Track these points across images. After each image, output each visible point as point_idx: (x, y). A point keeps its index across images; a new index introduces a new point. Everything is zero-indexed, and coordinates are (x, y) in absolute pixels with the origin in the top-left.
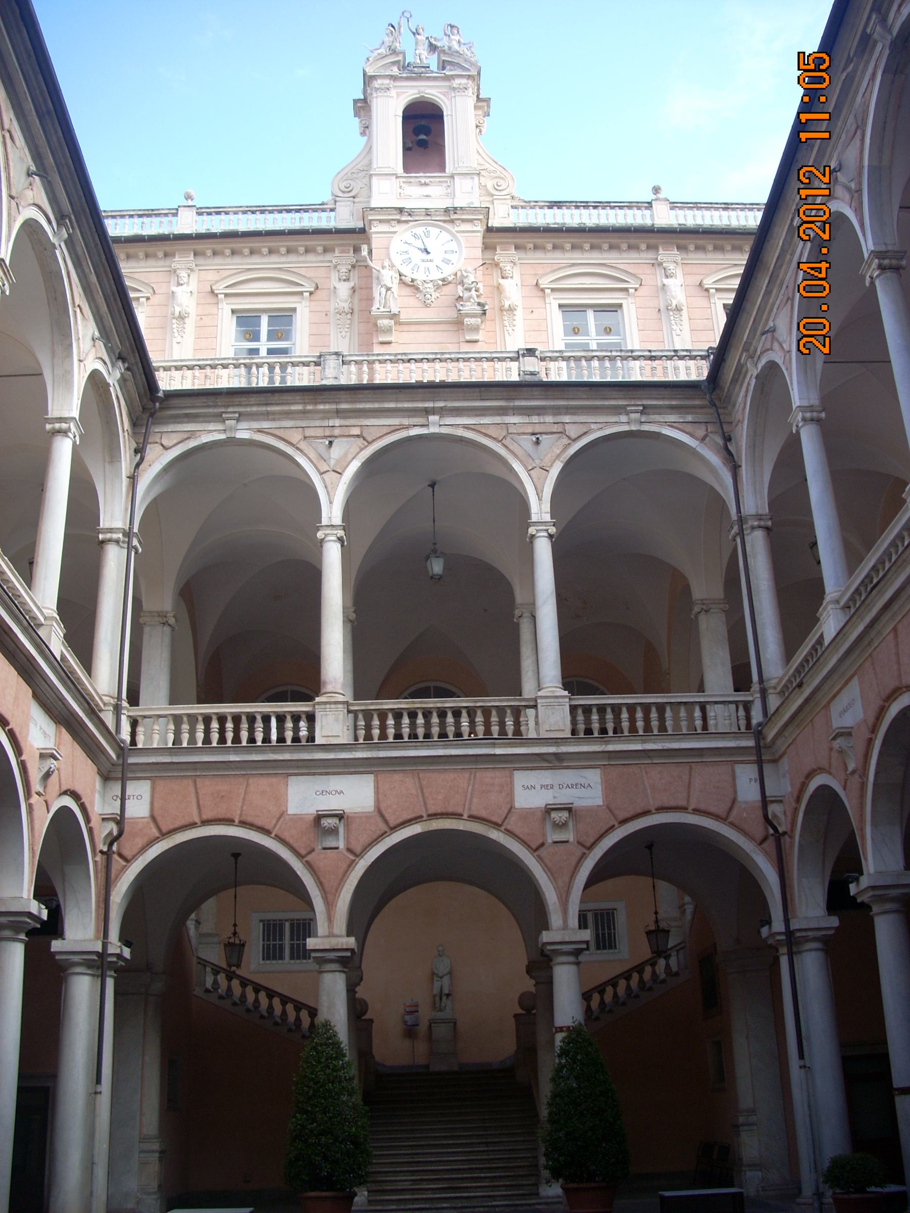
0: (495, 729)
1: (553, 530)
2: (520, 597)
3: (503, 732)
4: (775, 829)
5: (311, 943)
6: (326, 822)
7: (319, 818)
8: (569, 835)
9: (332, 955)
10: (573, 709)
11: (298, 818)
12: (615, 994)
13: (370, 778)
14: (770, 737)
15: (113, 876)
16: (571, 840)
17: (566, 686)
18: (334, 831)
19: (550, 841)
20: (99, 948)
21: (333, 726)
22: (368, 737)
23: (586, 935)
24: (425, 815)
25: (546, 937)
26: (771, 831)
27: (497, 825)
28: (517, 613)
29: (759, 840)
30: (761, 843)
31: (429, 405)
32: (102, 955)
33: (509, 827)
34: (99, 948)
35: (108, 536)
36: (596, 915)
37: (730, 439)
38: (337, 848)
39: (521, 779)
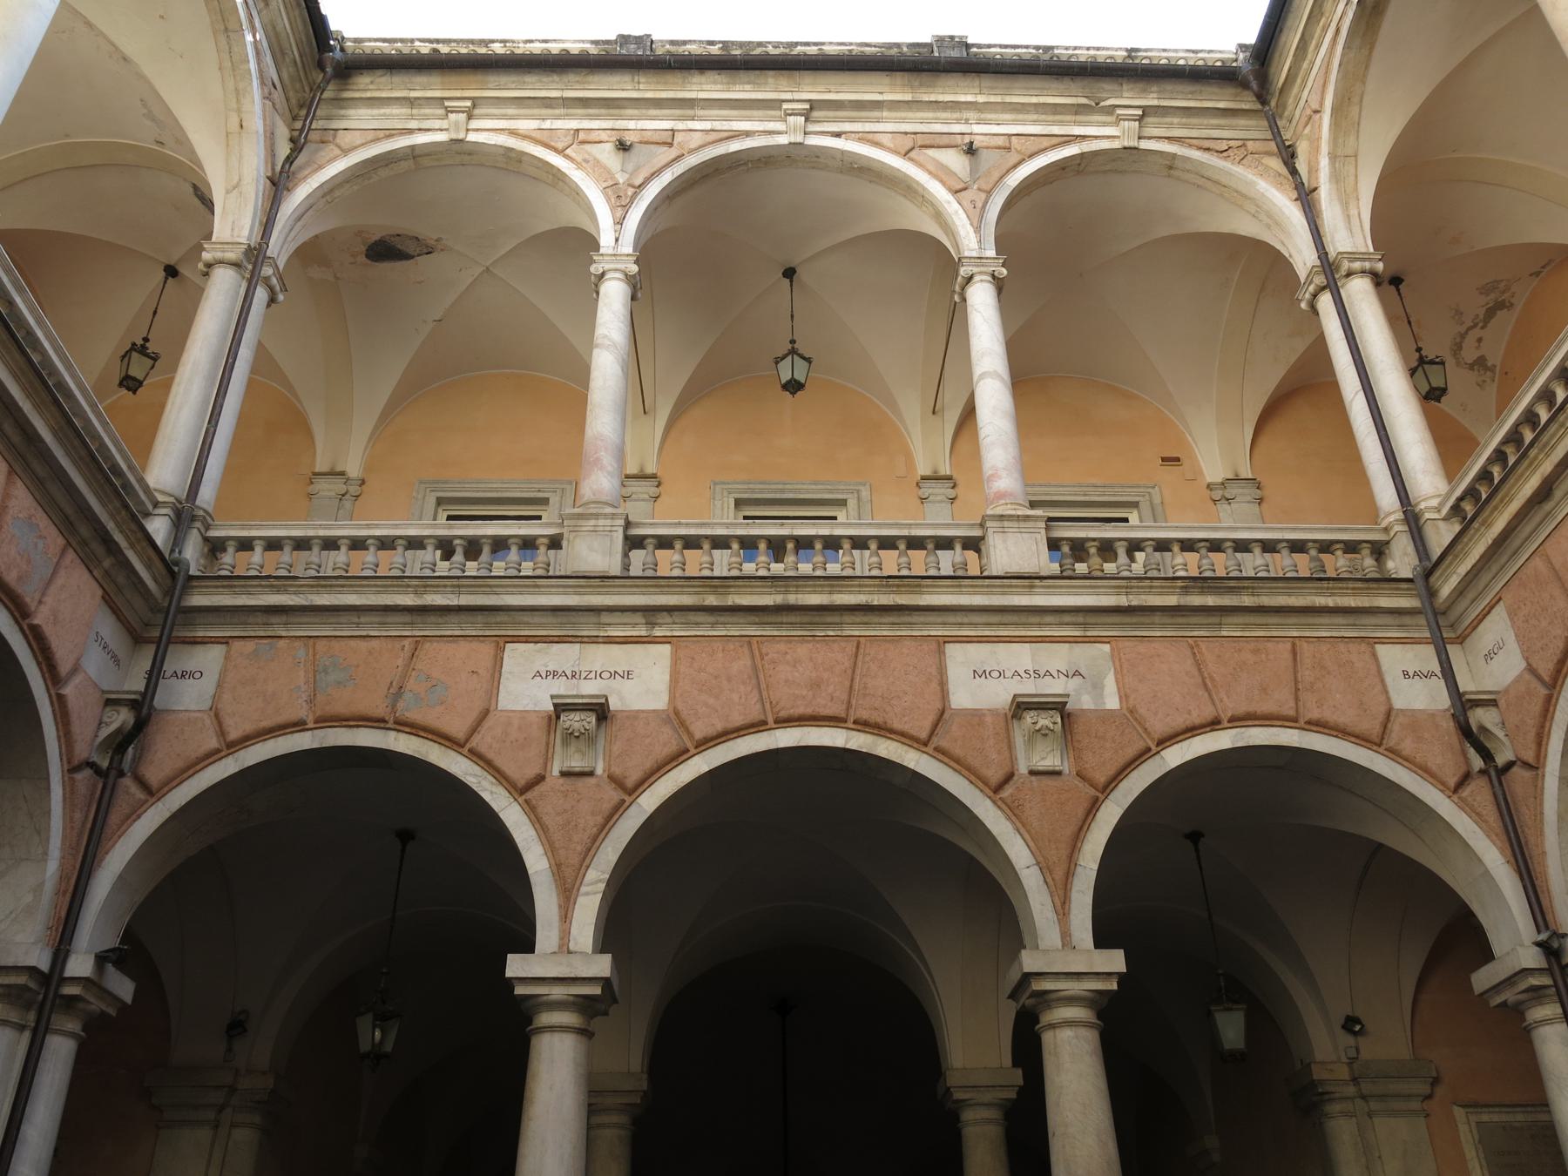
4: (1487, 755)
5: (516, 966)
6: (573, 721)
9: (558, 992)
13: (666, 649)
14: (1445, 591)
15: (114, 818)
16: (1066, 771)
19: (1023, 769)
20: (44, 964)
23: (1115, 961)
24: (770, 720)
25: (1030, 961)
26: (1478, 763)
29: (1452, 782)
30: (1456, 789)
32: (50, 979)
33: (944, 744)
34: (44, 964)
37: (1293, 156)
38: (591, 774)
39: (961, 660)
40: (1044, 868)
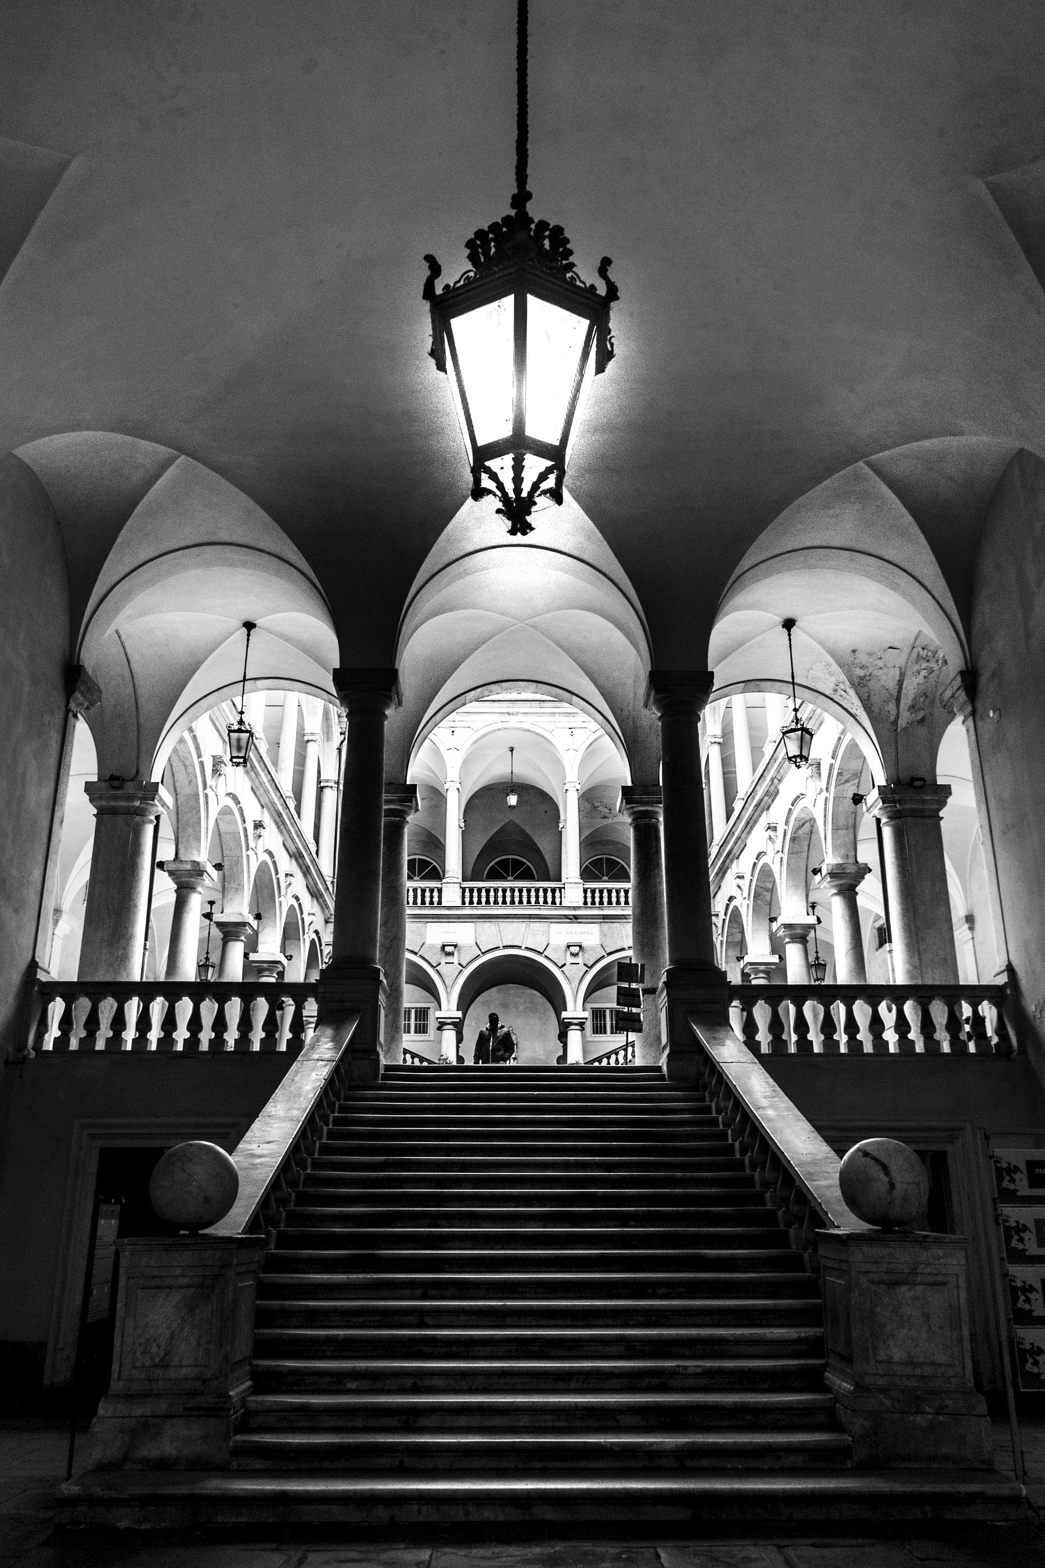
0: (541, 900)
1: (579, 787)
2: (562, 817)
3: (545, 902)
7: (443, 946)
8: (579, 960)
9: (449, 1021)
10: (585, 891)
11: (433, 946)
12: (617, 1060)
17: (582, 877)
18: (451, 954)
19: (568, 963)
21: (452, 895)
22: (471, 902)
25: (564, 1015)
27: (540, 953)
28: (561, 825)
31: (510, 710)
35: (326, 784)
36: (611, 1012)
40: (572, 989)
